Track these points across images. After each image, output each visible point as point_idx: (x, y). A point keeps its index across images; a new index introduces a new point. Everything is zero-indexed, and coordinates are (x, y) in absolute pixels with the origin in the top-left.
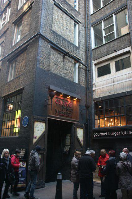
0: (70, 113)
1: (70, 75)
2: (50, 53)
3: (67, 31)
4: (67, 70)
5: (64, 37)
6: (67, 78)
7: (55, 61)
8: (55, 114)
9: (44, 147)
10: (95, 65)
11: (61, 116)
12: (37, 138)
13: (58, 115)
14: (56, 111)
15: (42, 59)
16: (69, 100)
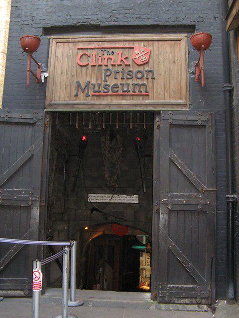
0: (140, 82)
14: (79, 85)
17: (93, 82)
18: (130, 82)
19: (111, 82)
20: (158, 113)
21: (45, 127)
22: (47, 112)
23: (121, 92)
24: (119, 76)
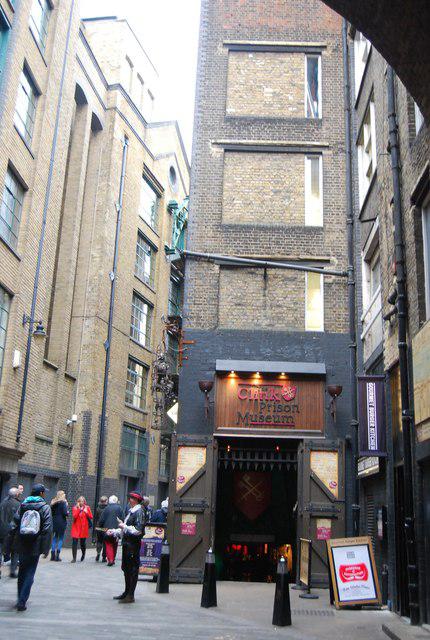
0: (288, 415)
1: (290, 317)
2: (218, 286)
3: (277, 197)
4: (279, 306)
5: (265, 222)
6: (280, 327)
7: (236, 297)
8: (238, 425)
9: (206, 496)
10: (368, 261)
11: (255, 425)
12: (186, 481)
13: (246, 426)
14: (240, 416)
15: (194, 308)
16: (283, 383)
17: (252, 413)
18: (279, 414)
19: (266, 414)
20: (302, 440)
21: (215, 448)
22: (215, 437)
23: (272, 422)
24: (272, 409)
